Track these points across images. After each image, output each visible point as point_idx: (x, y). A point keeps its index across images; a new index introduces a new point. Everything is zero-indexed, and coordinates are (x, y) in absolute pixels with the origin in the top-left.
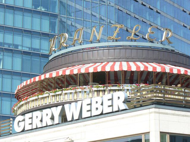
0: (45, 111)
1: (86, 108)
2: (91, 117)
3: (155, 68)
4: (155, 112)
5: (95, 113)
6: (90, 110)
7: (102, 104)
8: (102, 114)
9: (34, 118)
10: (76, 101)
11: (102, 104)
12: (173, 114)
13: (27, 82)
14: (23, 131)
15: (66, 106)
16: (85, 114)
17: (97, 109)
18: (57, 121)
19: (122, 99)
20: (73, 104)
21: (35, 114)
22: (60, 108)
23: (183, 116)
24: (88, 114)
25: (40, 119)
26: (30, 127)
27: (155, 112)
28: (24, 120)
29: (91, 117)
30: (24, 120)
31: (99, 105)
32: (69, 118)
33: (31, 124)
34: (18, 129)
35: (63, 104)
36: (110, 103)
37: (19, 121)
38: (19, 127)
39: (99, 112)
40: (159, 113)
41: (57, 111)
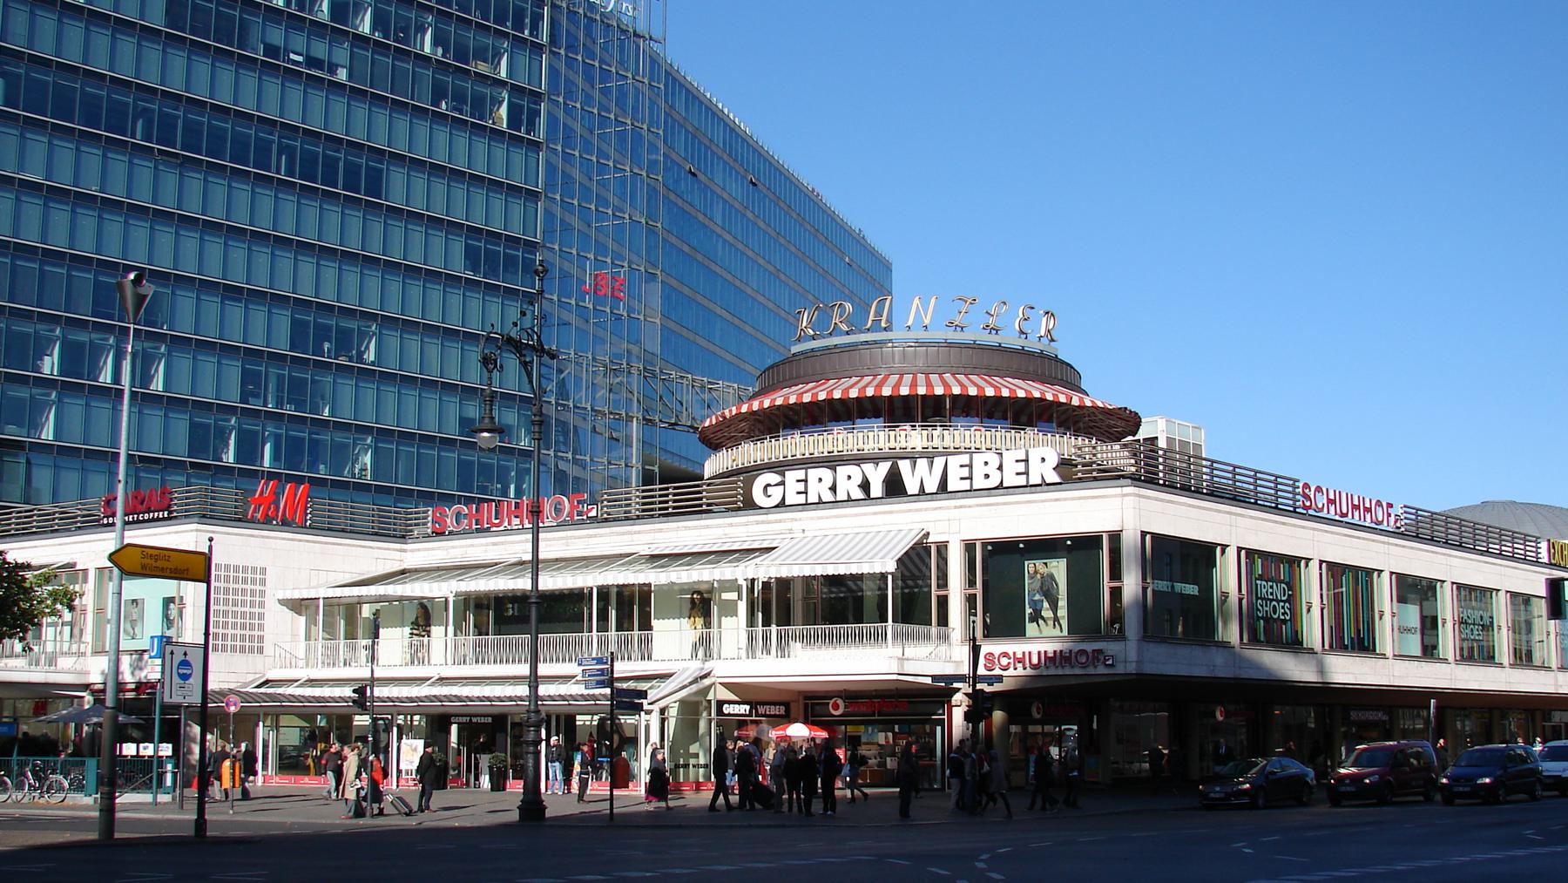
0: (842, 471)
2: (970, 491)
5: (979, 483)
7: (1000, 468)
8: (1000, 486)
11: (1000, 468)
12: (1156, 499)
14: (782, 504)
15: (904, 466)
17: (987, 476)
18: (877, 490)
19: (1053, 460)
21: (814, 474)
23: (1169, 501)
24: (966, 485)
29: (970, 491)
30: (782, 483)
31: (992, 469)
32: (912, 486)
35: (894, 457)
36: (1021, 467)
39: (994, 482)
40: (1140, 496)
41: (877, 475)
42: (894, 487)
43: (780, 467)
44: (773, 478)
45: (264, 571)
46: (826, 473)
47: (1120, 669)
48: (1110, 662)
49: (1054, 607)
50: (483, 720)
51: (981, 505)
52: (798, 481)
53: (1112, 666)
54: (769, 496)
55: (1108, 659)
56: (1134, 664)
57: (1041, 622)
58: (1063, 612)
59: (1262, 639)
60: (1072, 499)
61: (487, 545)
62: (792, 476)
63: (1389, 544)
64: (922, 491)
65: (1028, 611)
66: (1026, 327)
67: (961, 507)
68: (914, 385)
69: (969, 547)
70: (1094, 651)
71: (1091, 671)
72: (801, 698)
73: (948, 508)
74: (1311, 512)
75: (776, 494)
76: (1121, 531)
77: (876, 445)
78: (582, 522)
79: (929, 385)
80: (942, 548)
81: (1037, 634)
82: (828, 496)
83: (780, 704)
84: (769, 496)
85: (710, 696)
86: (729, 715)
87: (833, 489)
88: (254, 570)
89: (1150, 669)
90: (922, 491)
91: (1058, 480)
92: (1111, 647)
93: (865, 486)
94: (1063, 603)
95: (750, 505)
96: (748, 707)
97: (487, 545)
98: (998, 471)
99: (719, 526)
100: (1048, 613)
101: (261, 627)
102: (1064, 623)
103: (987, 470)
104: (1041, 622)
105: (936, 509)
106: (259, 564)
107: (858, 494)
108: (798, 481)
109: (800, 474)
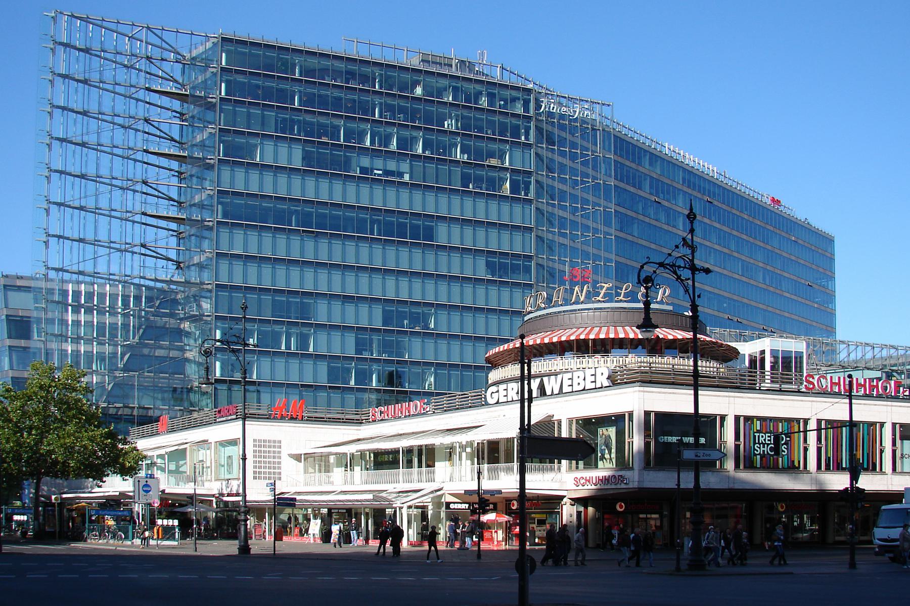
1: (566, 383)
2: (573, 392)
4: (639, 391)
5: (576, 388)
7: (584, 379)
8: (584, 390)
9: (510, 389)
11: (584, 379)
13: (499, 349)
14: (498, 402)
15: (545, 379)
16: (566, 389)
20: (553, 378)
24: (570, 389)
26: (505, 399)
27: (639, 391)
28: (498, 391)
30: (498, 391)
31: (581, 380)
32: (548, 392)
33: (506, 396)
34: (490, 401)
36: (593, 379)
37: (493, 393)
38: (492, 398)
40: (644, 392)
45: (280, 442)
47: (631, 486)
48: (625, 482)
49: (610, 453)
53: (626, 483)
56: (637, 483)
57: (604, 460)
58: (613, 455)
59: (758, 466)
62: (502, 387)
65: (599, 455)
68: (608, 333)
70: (619, 476)
71: (618, 486)
77: (548, 369)
79: (616, 333)
81: (602, 467)
83: (467, 503)
85: (443, 500)
86: (454, 509)
88: (274, 442)
89: (647, 484)
94: (614, 450)
95: (487, 404)
96: (467, 506)
100: (607, 456)
101: (279, 468)
102: (614, 461)
104: (604, 460)
106: (279, 439)
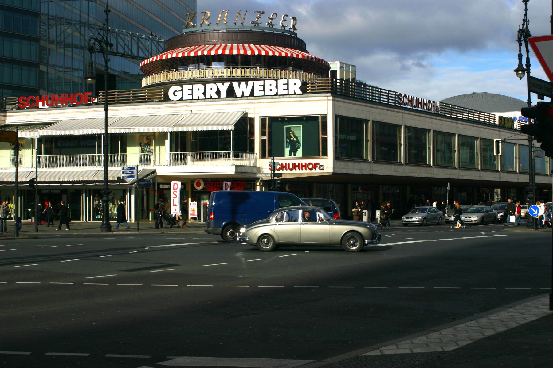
0: (208, 86)
3: (303, 56)
5: (267, 93)
6: (264, 90)
7: (277, 87)
8: (276, 94)
10: (247, 80)
14: (181, 99)
15: (235, 84)
17: (271, 90)
18: (223, 94)
20: (243, 84)
21: (196, 87)
22: (227, 85)
24: (262, 94)
25: (203, 91)
30: (182, 90)
31: (273, 87)
32: (238, 93)
35: (231, 80)
36: (286, 87)
39: (274, 92)
41: (224, 88)
42: (231, 93)
43: (181, 83)
44: (178, 88)
46: (201, 87)
47: (325, 171)
48: (322, 168)
50: (56, 192)
51: (268, 102)
52: (189, 90)
54: (176, 96)
55: (321, 167)
60: (307, 101)
61: (46, 114)
62: (186, 87)
63: (433, 118)
64: (243, 96)
66: (285, 24)
67: (260, 103)
69: (263, 120)
70: (315, 163)
72: (190, 182)
73: (254, 103)
74: (402, 106)
75: (179, 95)
76: (327, 114)
78: (91, 105)
80: (252, 120)
82: (202, 97)
84: (176, 96)
87: (204, 93)
90: (243, 96)
91: (301, 93)
92: (321, 161)
93: (218, 92)
97: (46, 114)
98: (276, 88)
99: (153, 108)
103: (271, 87)
105: (249, 103)
107: (215, 96)
108: (189, 90)
109: (190, 87)
